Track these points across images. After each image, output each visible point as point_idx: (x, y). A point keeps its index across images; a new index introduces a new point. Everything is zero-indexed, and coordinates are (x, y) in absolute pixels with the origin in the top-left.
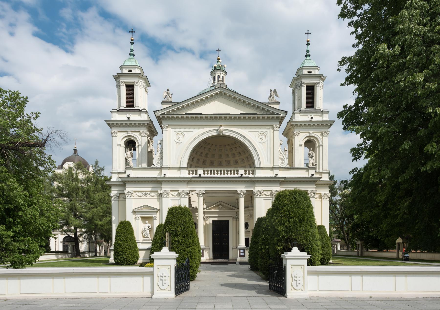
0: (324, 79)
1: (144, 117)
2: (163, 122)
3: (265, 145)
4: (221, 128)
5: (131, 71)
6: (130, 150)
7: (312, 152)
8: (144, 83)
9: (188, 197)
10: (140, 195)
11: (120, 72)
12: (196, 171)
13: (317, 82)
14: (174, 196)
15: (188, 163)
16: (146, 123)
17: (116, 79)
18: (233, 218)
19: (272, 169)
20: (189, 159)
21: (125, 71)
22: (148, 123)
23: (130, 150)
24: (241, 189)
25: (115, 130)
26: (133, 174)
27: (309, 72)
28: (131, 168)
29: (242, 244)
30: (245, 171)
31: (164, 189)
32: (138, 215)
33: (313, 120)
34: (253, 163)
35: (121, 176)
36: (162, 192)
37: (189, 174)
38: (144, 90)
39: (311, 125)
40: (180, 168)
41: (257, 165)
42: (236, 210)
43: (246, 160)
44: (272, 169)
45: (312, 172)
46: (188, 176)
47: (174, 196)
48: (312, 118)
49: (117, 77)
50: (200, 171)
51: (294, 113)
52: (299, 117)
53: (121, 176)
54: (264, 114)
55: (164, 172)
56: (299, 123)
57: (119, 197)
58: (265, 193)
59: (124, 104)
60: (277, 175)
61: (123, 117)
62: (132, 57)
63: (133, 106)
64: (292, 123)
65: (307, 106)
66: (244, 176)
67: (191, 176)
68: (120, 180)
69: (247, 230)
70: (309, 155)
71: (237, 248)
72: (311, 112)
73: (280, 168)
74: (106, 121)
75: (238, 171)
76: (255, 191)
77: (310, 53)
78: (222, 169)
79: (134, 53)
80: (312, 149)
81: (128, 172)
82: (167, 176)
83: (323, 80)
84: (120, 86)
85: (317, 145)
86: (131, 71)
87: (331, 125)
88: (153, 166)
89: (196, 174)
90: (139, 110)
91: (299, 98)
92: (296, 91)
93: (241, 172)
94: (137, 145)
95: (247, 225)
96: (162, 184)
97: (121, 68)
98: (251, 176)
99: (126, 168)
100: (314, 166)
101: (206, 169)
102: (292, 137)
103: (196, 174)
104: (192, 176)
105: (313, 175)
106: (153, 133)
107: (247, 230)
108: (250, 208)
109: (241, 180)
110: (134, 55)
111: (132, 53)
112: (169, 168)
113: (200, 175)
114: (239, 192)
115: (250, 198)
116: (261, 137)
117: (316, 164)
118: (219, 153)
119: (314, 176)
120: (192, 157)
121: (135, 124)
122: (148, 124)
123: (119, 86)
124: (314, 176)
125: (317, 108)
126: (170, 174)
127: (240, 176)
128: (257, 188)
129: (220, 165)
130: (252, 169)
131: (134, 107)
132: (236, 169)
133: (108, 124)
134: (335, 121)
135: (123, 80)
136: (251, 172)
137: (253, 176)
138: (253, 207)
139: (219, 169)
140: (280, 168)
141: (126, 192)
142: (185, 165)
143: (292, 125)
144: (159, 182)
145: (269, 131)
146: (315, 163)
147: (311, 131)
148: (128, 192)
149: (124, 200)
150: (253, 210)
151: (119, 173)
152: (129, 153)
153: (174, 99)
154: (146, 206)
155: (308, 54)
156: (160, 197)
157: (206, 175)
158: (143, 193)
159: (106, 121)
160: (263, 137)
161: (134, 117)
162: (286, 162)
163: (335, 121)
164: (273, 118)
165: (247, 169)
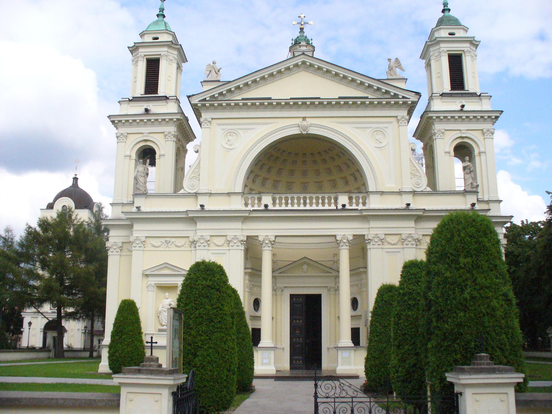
0: (478, 45)
1: (171, 108)
2: (203, 115)
3: (383, 151)
4: (305, 123)
5: (157, 38)
6: (144, 163)
7: (468, 163)
8: (176, 56)
9: (243, 248)
10: (156, 245)
11: (139, 40)
12: (260, 200)
13: (465, 49)
14: (217, 246)
15: (246, 186)
16: (175, 117)
17: (132, 52)
18: (329, 290)
19: (400, 193)
20: (247, 178)
21: (148, 39)
22: (179, 117)
23: (144, 163)
24: (345, 230)
25: (124, 130)
26: (148, 206)
27: (450, 34)
28: (145, 194)
29: (346, 340)
30: (350, 199)
31: (199, 233)
32: (153, 281)
33: (465, 109)
34: (365, 184)
35: (127, 209)
36: (196, 239)
37: (246, 205)
38: (175, 66)
39: (462, 116)
40: (229, 194)
41: (371, 188)
42: (335, 274)
43: (351, 179)
44: (400, 193)
45: (472, 199)
46: (244, 208)
47: (217, 246)
48: (463, 106)
49: (134, 49)
50: (267, 199)
51: (431, 98)
52: (438, 105)
53: (127, 209)
54: (383, 96)
55: (202, 200)
56: (442, 115)
57: (121, 248)
58: (389, 239)
59: (140, 90)
60: (408, 205)
61: (138, 109)
62: (161, 18)
63: (156, 92)
64: (430, 115)
65: (453, 88)
66: (348, 207)
67: (250, 208)
68: (123, 216)
69: (355, 313)
70: (464, 168)
71: (337, 348)
72: (462, 95)
73: (414, 193)
74: (109, 117)
75: (336, 199)
76: (370, 237)
77: (449, 7)
78: (308, 196)
79: (165, 13)
80: (467, 158)
81: (139, 202)
82: (206, 208)
83: (476, 46)
84: (137, 62)
85: (476, 152)
86: (157, 38)
87: (497, 118)
88: (182, 191)
89: (259, 205)
90: (166, 96)
91: (439, 75)
92: (433, 63)
93: (343, 199)
94: (157, 156)
95: (354, 303)
96: (196, 223)
97: (142, 35)
98: (361, 207)
99: (135, 195)
100: (475, 190)
101: (277, 196)
102: (431, 138)
103: (259, 205)
104: (252, 209)
105: (473, 205)
106: (185, 134)
107: (355, 313)
108: (361, 270)
109: (342, 214)
110: (164, 17)
111: (161, 13)
112: (210, 194)
113: (266, 206)
114: (338, 238)
115: (360, 248)
116: (378, 137)
117: (478, 186)
118: (303, 164)
119: (477, 207)
120: (252, 175)
121: (157, 120)
122: (178, 119)
123: (135, 62)
124: (477, 207)
125: (471, 91)
126: (211, 205)
127: (340, 207)
128: (372, 230)
129: (305, 189)
130: (364, 195)
131: (157, 93)
132: (333, 196)
133: (113, 122)
134: (502, 111)
135: (143, 51)
136: (361, 201)
137: (364, 208)
138: (366, 267)
139: (302, 196)
140: (414, 193)
141: (132, 239)
142: (239, 189)
143: (431, 117)
144: (190, 219)
145: (391, 127)
146: (475, 184)
147: (463, 127)
148: (137, 238)
149: (129, 253)
150: (366, 273)
151: (123, 204)
152: (141, 168)
153: (224, 77)
154: (166, 266)
155: (446, 8)
156: (193, 248)
157: (277, 207)
158: (163, 240)
159: (109, 117)
160: (379, 136)
161: (156, 108)
162: (424, 181)
163: (502, 111)
164: (396, 103)
165: (354, 196)
